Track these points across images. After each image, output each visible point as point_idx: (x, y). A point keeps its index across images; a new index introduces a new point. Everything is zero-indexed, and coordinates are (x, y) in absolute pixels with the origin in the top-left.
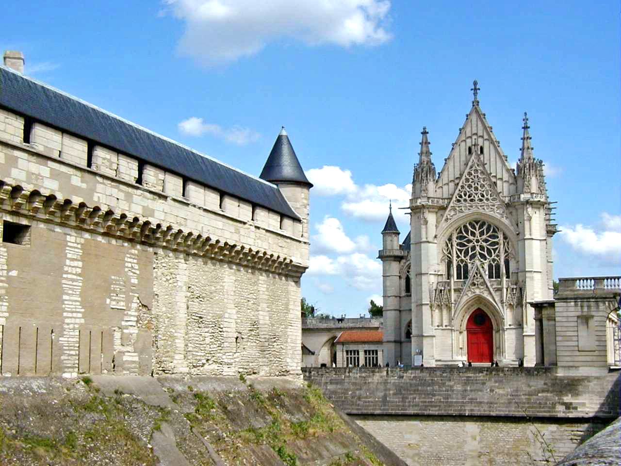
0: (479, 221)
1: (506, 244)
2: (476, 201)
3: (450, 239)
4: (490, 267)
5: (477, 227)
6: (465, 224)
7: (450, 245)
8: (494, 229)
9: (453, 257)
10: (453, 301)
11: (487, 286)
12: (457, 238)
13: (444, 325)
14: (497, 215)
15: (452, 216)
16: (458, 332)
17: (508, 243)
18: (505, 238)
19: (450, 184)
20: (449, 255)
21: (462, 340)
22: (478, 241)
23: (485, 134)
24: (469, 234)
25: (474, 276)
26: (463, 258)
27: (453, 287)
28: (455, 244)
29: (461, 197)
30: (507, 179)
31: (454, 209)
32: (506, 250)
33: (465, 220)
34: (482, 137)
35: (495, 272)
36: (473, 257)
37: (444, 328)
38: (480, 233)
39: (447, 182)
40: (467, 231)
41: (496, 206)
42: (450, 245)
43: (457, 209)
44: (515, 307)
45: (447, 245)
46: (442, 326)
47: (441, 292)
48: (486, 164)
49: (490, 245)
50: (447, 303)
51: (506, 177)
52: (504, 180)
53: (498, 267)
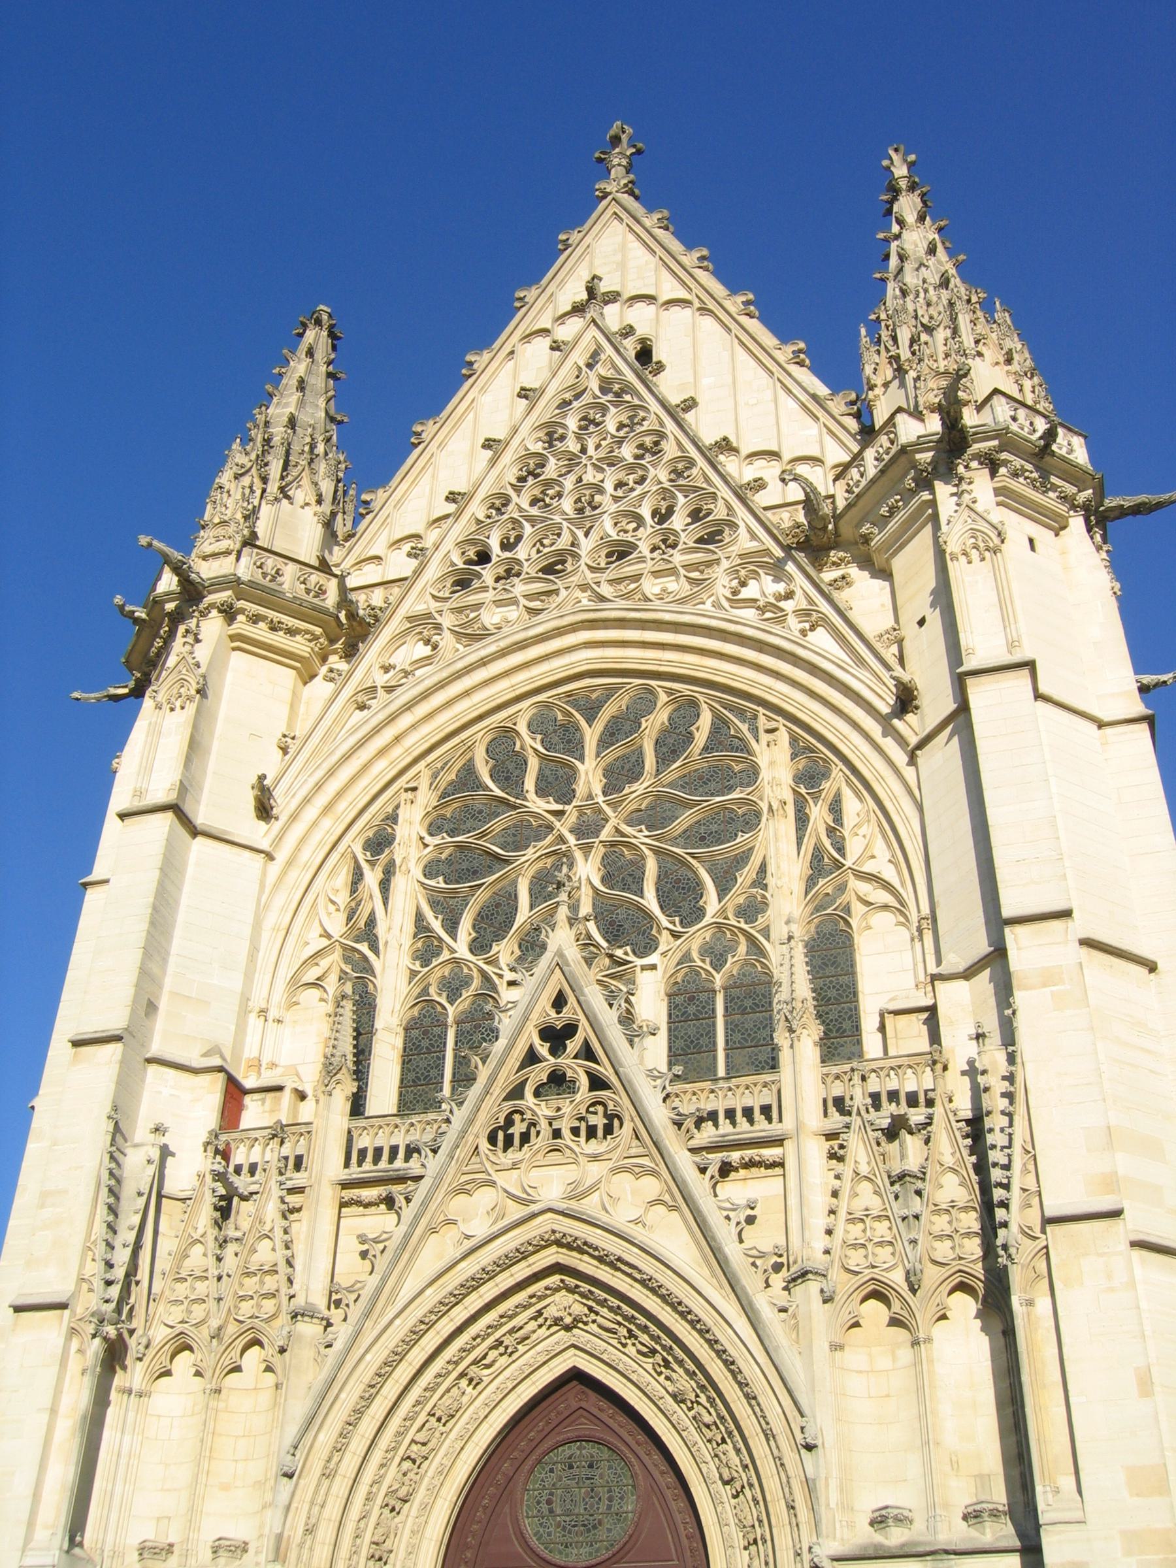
2: (585, 559)
5: (591, 735)
7: (372, 878)
14: (750, 614)
20: (364, 948)
24: (530, 784)
25: (532, 1057)
32: (818, 855)
33: (503, 690)
38: (608, 772)
40: (508, 766)
41: (725, 564)
42: (372, 878)
45: (357, 876)
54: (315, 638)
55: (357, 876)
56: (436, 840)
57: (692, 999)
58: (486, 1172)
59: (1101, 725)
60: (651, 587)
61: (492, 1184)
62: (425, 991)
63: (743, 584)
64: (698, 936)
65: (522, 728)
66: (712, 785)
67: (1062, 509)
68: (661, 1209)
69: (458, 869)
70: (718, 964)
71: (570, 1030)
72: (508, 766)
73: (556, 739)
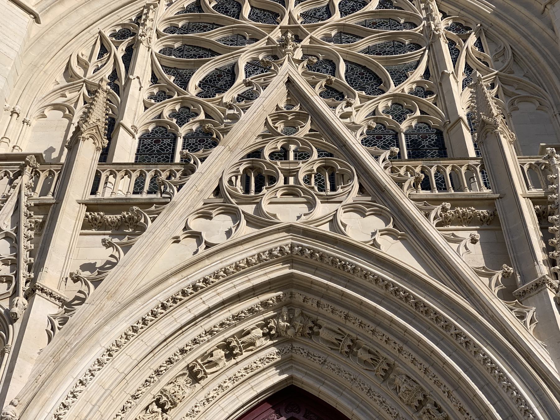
55: (104, 50)
58: (227, 200)
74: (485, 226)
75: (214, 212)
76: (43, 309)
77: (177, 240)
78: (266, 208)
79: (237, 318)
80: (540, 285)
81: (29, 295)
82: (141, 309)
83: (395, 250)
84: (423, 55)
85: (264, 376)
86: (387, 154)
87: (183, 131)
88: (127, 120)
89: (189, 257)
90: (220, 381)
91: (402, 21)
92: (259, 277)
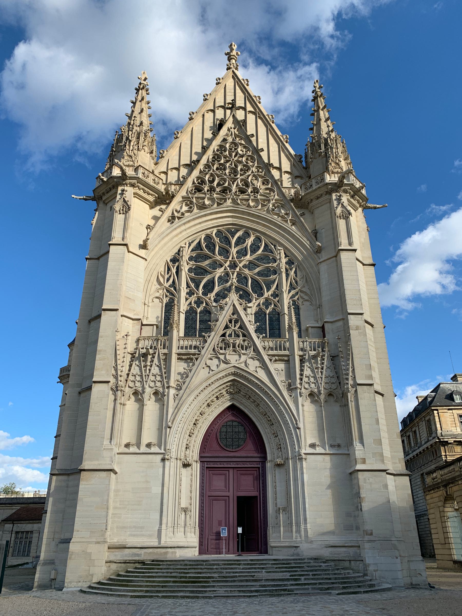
0: (238, 231)
1: (292, 273)
3: (175, 260)
4: (259, 316)
5: (233, 241)
6: (208, 232)
7: (174, 271)
8: (266, 245)
9: (179, 291)
10: (173, 383)
11: (256, 350)
12: (191, 259)
13: (145, 440)
15: (183, 214)
16: (180, 464)
17: (295, 272)
18: (290, 263)
19: (182, 169)
20: (172, 289)
21: (186, 486)
22: (233, 266)
23: (248, 105)
25: (227, 327)
26: (200, 294)
27: (175, 350)
28: (185, 268)
29: (203, 182)
30: (290, 171)
31: (187, 200)
33: (210, 224)
34: (244, 109)
35: (271, 324)
36: (222, 296)
37: (143, 449)
38: (237, 252)
39: (177, 166)
40: (211, 245)
41: (271, 202)
43: (194, 200)
44: (322, 397)
45: (169, 269)
46: (138, 445)
47: (145, 361)
48: (253, 135)
49: (259, 274)
50: (159, 384)
51: (286, 166)
52: (283, 170)
53: (276, 317)
54: (156, 197)
55: (169, 269)
56: (191, 263)
57: (260, 315)
58: (216, 354)
59: (364, 265)
60: (252, 204)
61: (218, 358)
62: (190, 303)
63: (275, 208)
64: (262, 300)
65: (214, 235)
66: (264, 261)
67: (358, 205)
68: (260, 369)
69: (198, 272)
70: (267, 308)
71: (236, 322)
72: (211, 245)
73: (223, 240)
74: (286, 362)
75: (213, 358)
76: (172, 392)
77: (204, 368)
78: (228, 357)
79: (220, 390)
80: (296, 388)
81: (168, 387)
82: (196, 392)
83: (262, 375)
84: (277, 277)
85: (226, 403)
86: (261, 336)
87: (199, 310)
88: (181, 310)
89: (208, 375)
90: (215, 406)
91: (271, 258)
92: (226, 380)
